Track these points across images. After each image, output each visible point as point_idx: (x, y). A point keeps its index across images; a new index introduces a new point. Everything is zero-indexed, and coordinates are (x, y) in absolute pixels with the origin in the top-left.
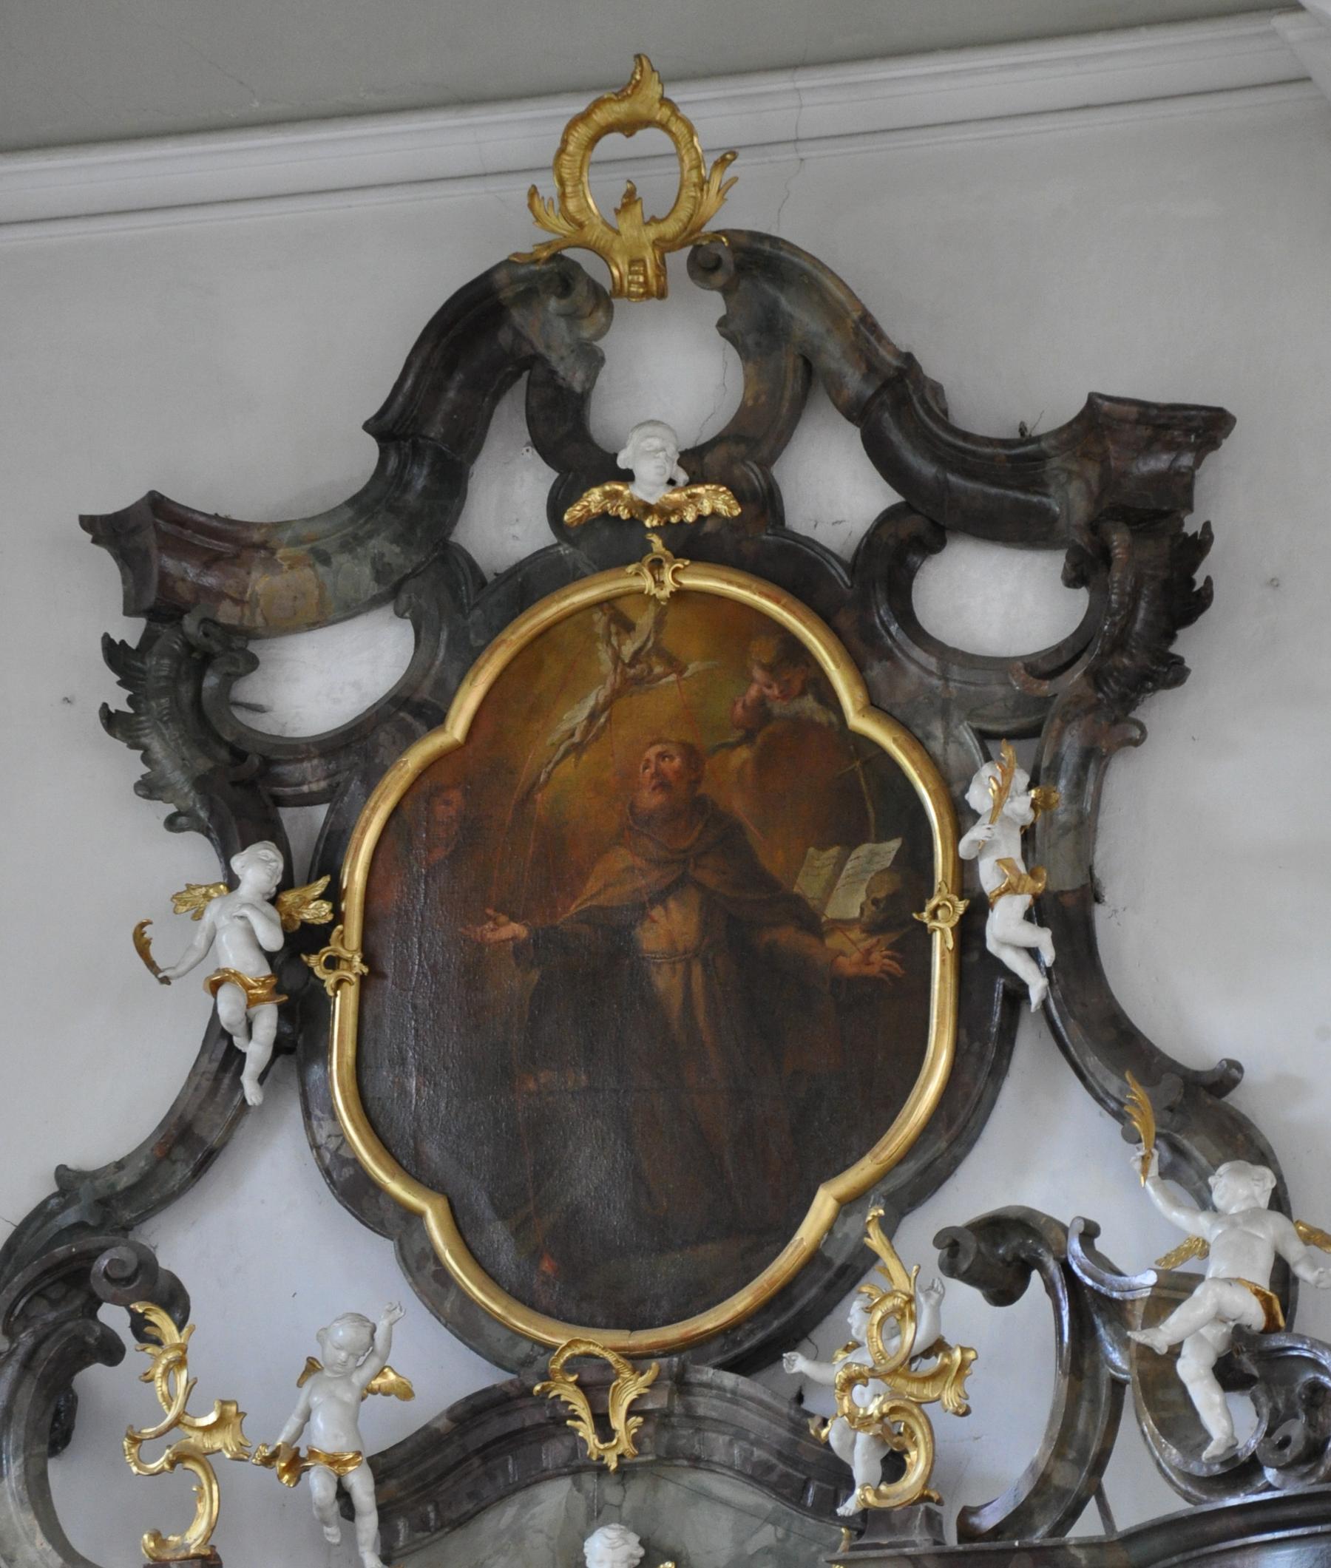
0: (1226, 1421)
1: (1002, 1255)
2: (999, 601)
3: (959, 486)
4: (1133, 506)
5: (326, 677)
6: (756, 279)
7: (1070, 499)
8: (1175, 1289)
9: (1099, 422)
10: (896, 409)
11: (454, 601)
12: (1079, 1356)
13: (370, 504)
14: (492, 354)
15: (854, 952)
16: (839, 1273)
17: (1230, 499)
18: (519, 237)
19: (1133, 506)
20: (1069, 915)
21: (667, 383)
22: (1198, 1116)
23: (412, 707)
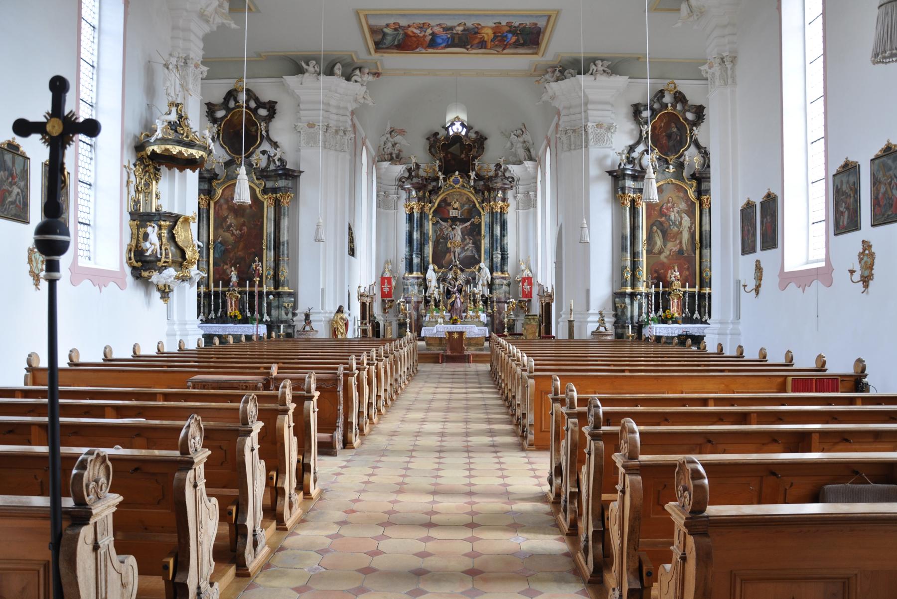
0: (278, 163)
1: (264, 152)
2: (263, 112)
3: (260, 105)
4: (271, 107)
5: (220, 114)
6: (248, 91)
7: (268, 106)
8: (275, 155)
9: (270, 102)
10: (257, 100)
11: (228, 110)
12: (269, 159)
13: (223, 103)
14: (231, 95)
15: (254, 133)
16: (252, 153)
17: (277, 107)
18: (233, 87)
19: (271, 107)
20: (267, 131)
21: (243, 97)
22: (275, 145)
23: (225, 116)
